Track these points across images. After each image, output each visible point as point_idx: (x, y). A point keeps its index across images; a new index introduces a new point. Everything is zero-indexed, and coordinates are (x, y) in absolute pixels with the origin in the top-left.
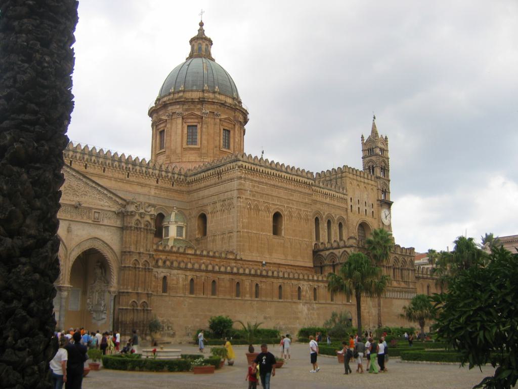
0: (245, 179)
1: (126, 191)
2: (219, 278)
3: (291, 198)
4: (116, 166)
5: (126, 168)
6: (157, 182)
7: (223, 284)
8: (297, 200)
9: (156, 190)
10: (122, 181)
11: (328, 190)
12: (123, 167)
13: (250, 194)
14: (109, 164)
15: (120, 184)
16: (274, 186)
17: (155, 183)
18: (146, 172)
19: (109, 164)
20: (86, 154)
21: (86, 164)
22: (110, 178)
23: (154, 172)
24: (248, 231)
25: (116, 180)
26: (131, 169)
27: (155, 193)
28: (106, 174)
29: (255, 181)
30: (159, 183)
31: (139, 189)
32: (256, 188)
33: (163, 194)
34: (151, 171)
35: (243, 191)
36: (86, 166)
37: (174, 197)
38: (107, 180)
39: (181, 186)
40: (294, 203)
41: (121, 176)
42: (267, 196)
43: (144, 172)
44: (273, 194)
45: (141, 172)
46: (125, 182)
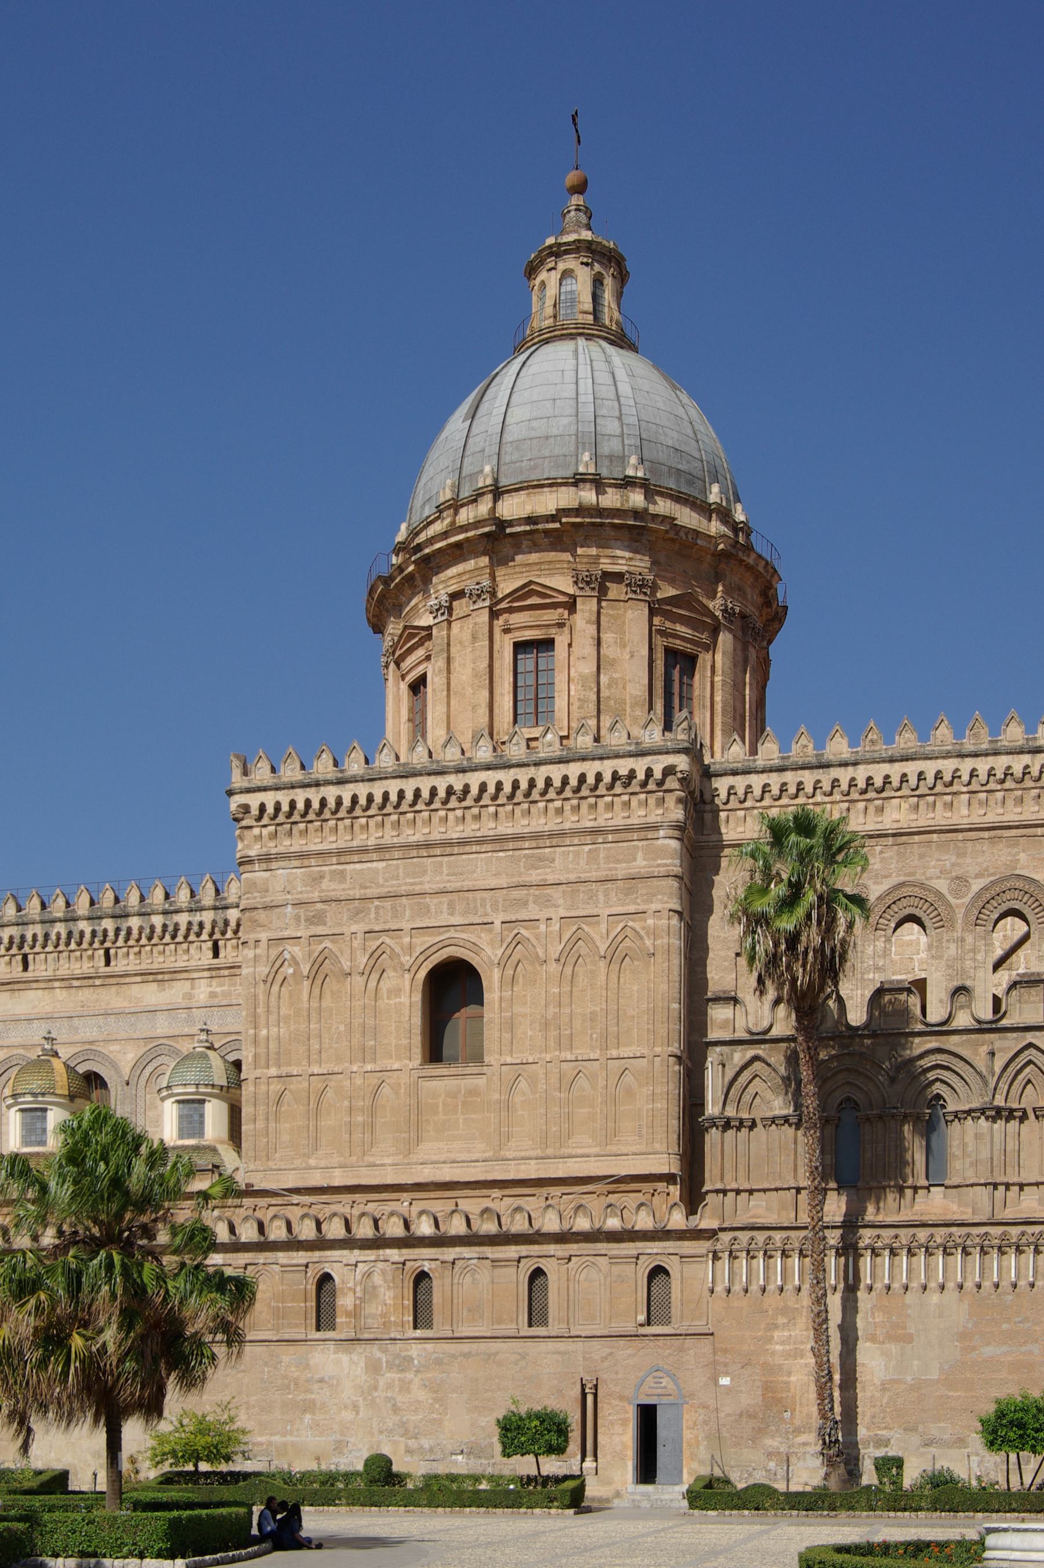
0: (266, 858)
3: (534, 876)
6: (216, 954)
8: (572, 877)
9: (214, 982)
10: (90, 982)
11: (892, 760)
13: (297, 918)
15: (85, 995)
16: (428, 846)
24: (284, 1070)
25: (68, 982)
27: (213, 995)
28: (29, 975)
29: (320, 854)
31: (150, 995)
32: (325, 884)
35: (261, 916)
38: (40, 991)
40: (556, 893)
42: (388, 904)
44: (427, 887)
46: (98, 982)
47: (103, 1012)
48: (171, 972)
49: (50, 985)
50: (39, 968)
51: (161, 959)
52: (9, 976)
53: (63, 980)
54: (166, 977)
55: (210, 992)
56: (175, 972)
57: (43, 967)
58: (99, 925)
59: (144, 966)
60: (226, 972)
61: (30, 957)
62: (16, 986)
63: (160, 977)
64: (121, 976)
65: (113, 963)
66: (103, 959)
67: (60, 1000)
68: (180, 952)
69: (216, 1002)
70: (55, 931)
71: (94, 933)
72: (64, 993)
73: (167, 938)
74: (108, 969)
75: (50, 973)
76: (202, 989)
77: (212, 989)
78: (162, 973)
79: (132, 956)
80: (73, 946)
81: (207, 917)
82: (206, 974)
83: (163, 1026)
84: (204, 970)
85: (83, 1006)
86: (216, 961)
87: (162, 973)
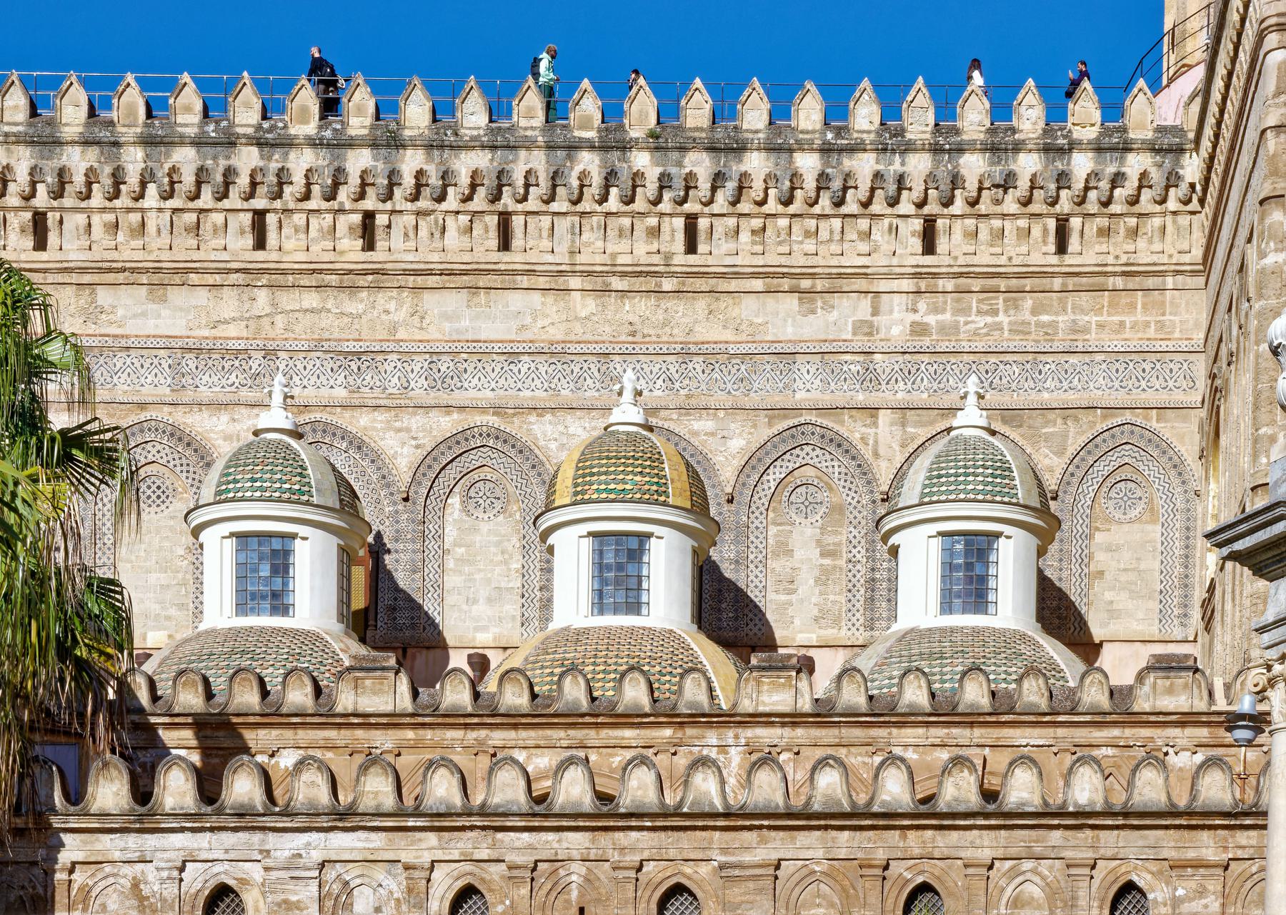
1: (686, 354)
6: (929, 246)
9: (922, 306)
10: (651, 283)
15: (638, 309)
27: (919, 329)
30: (942, 244)
37: (1075, 329)
38: (536, 296)
39: (1134, 233)
46: (668, 285)
47: (678, 347)
48: (830, 276)
51: (810, 246)
52: (467, 257)
53: (590, 273)
54: (820, 285)
55: (913, 324)
56: (840, 276)
57: (546, 244)
58: (680, 164)
59: (771, 259)
60: (949, 285)
61: (517, 222)
62: (483, 281)
63: (805, 284)
64: (723, 276)
65: (702, 248)
66: (680, 237)
68: (851, 235)
69: (926, 342)
70: (578, 169)
71: (664, 182)
73: (825, 203)
74: (692, 259)
75: (561, 257)
76: (896, 315)
77: (917, 317)
78: (813, 276)
79: (745, 237)
80: (613, 203)
82: (907, 285)
84: (901, 276)
85: (633, 334)
86: (929, 260)
87: (813, 276)
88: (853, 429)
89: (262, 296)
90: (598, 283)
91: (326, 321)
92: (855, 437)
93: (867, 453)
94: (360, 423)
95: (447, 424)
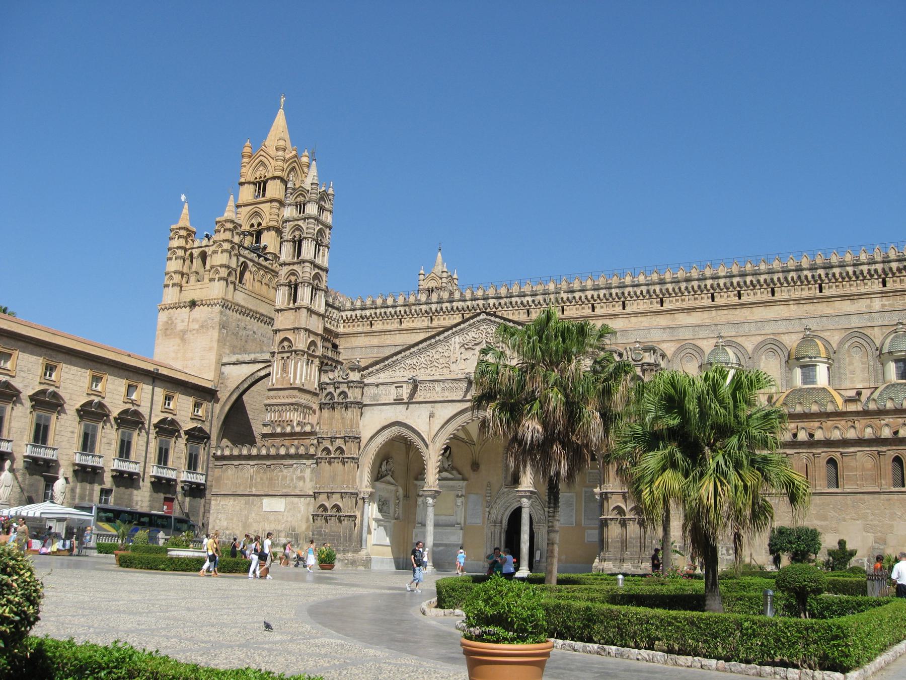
2: (841, 454)
4: (793, 278)
5: (813, 276)
7: (853, 464)
9: (884, 299)
10: (811, 301)
12: (806, 277)
14: (779, 279)
17: (877, 286)
18: (854, 273)
19: (779, 279)
20: (734, 276)
21: (739, 292)
22: (786, 302)
23: (873, 267)
25: (797, 301)
26: (823, 277)
27: (883, 306)
31: (847, 306)
33: (899, 302)
34: (865, 268)
36: (739, 296)
41: (806, 293)
43: (851, 273)
45: (846, 277)
46: (815, 301)
49: (787, 303)
50: (780, 295)
54: (855, 297)
60: (891, 294)
63: (852, 297)
67: (793, 310)
69: (886, 309)
70: (790, 275)
72: (796, 307)
74: (821, 294)
81: (879, 267)
83: (855, 322)
86: (885, 288)
88: (868, 332)
89: (714, 312)
90: (797, 302)
91: (729, 317)
92: (869, 335)
93: (872, 338)
94: (739, 340)
95: (760, 339)
